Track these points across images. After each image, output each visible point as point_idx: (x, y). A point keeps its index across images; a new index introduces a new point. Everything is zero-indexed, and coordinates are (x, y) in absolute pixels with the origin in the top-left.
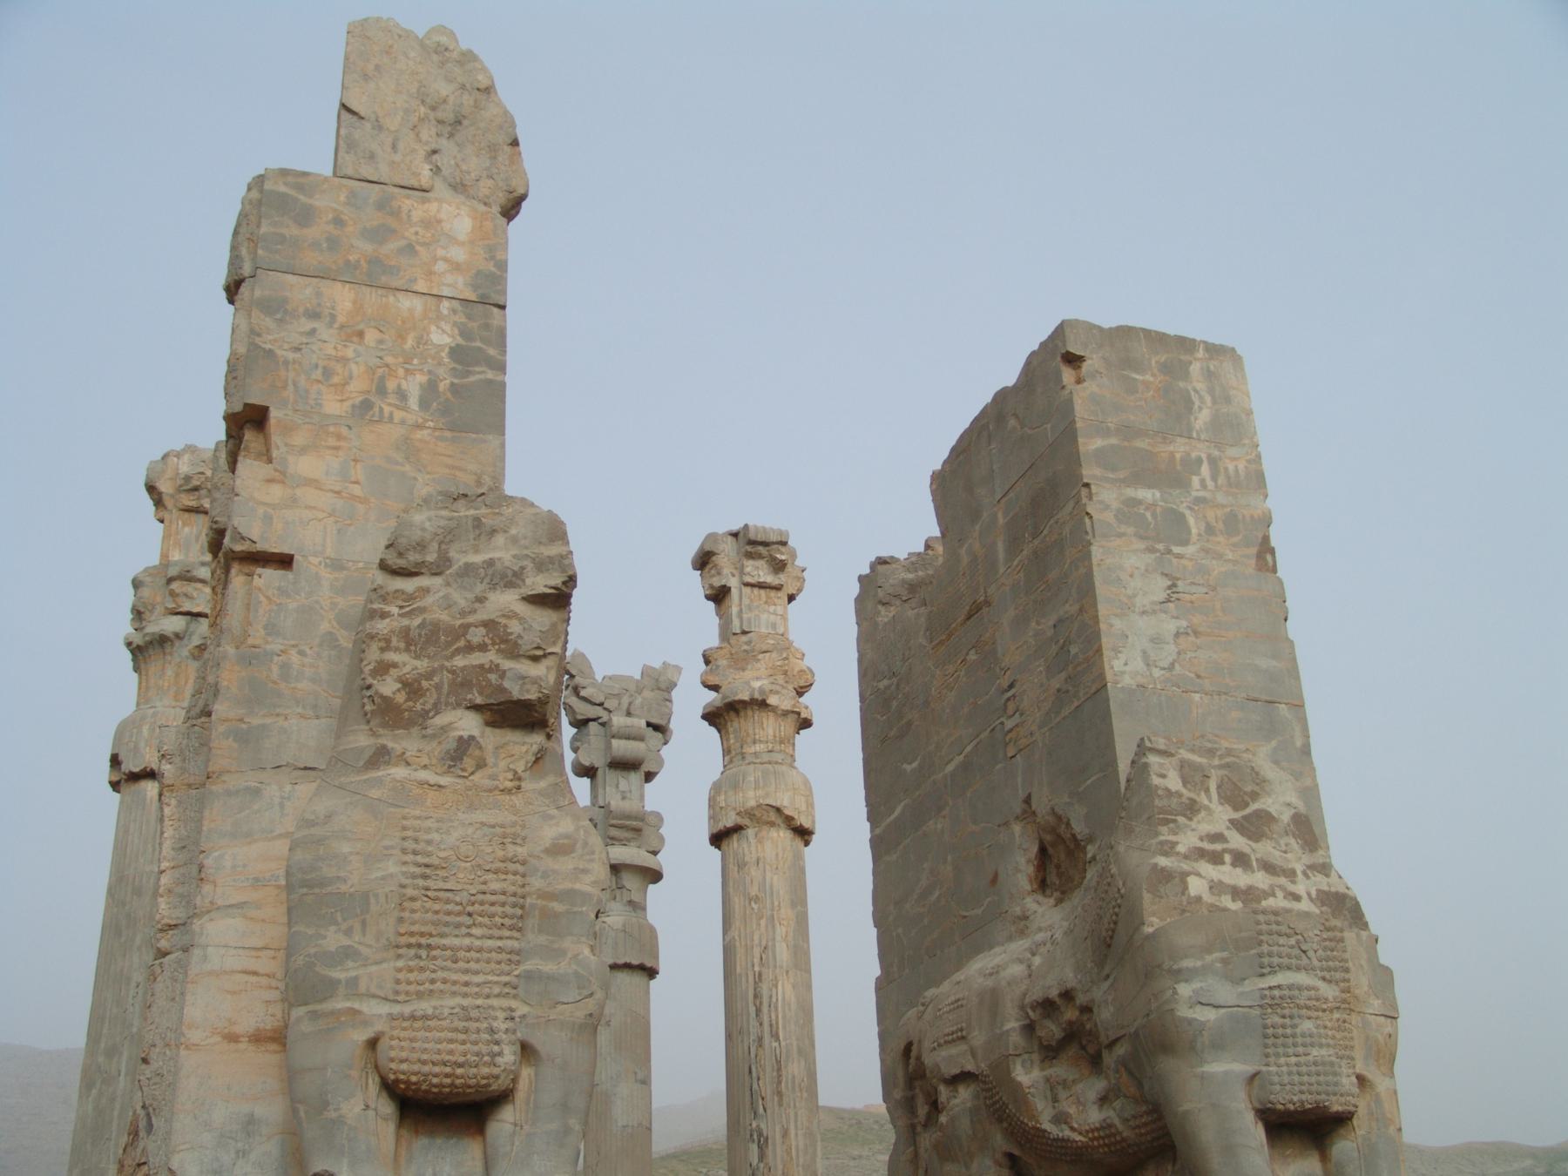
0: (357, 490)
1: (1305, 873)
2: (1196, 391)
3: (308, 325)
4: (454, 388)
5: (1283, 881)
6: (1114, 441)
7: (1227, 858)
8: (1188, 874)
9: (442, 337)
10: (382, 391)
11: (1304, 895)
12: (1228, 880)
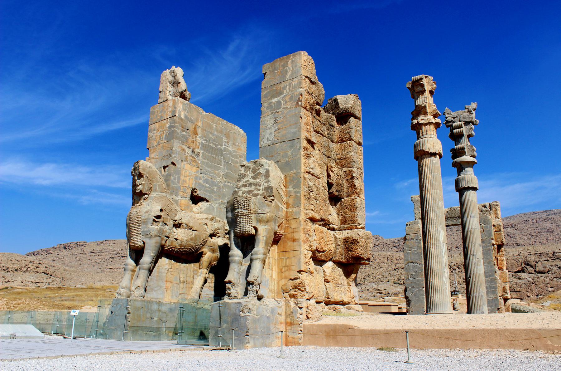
0: (157, 157)
1: (263, 185)
2: (289, 68)
3: (153, 132)
4: (169, 134)
5: (258, 187)
6: (268, 91)
7: (248, 185)
8: (239, 191)
9: (168, 126)
10: (161, 139)
11: (261, 189)
12: (246, 190)
